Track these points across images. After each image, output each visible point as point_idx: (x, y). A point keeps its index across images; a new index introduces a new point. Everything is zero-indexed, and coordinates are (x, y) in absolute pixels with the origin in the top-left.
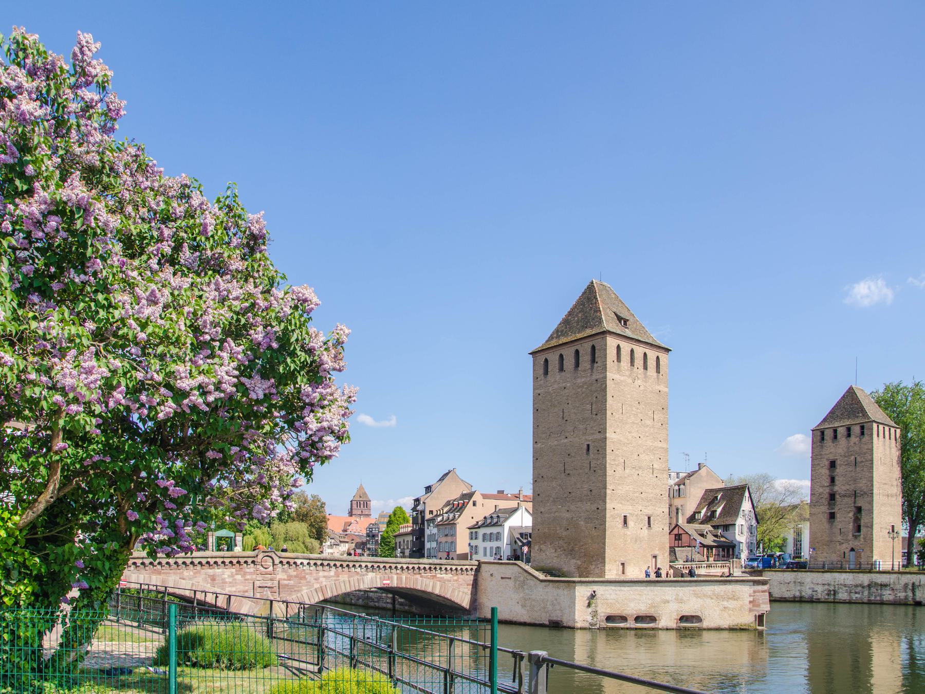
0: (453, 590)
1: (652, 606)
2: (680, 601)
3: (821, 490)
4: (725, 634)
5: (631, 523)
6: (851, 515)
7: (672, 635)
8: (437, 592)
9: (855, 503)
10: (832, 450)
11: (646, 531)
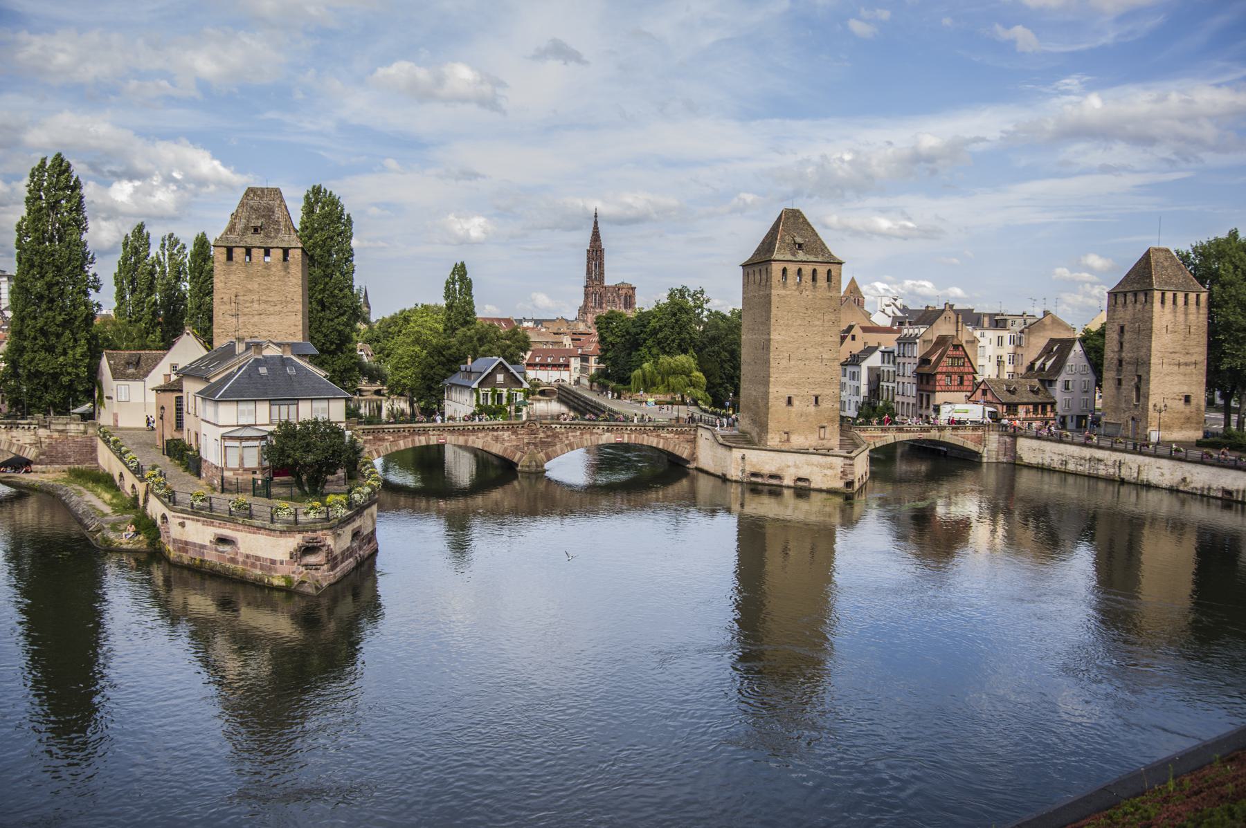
0: (675, 445)
1: (779, 469)
2: (796, 466)
3: (1112, 355)
4: (824, 495)
5: (796, 402)
6: (1133, 383)
7: (792, 491)
8: (661, 446)
9: (1136, 371)
10: (1121, 316)
11: (813, 408)
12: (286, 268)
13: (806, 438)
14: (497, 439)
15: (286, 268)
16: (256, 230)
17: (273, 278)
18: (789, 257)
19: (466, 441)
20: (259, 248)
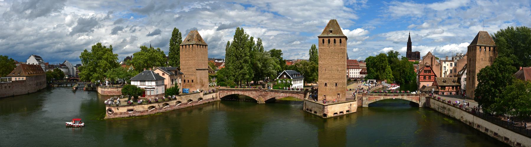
1: (312, 108)
5: (328, 85)
6: (472, 79)
8: (299, 98)
12: (193, 49)
13: (333, 98)
14: (252, 93)
15: (193, 49)
16: (188, 40)
17: (190, 52)
18: (326, 35)
19: (244, 93)
20: (188, 45)
